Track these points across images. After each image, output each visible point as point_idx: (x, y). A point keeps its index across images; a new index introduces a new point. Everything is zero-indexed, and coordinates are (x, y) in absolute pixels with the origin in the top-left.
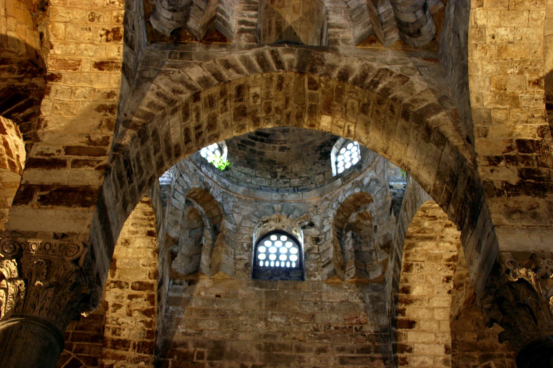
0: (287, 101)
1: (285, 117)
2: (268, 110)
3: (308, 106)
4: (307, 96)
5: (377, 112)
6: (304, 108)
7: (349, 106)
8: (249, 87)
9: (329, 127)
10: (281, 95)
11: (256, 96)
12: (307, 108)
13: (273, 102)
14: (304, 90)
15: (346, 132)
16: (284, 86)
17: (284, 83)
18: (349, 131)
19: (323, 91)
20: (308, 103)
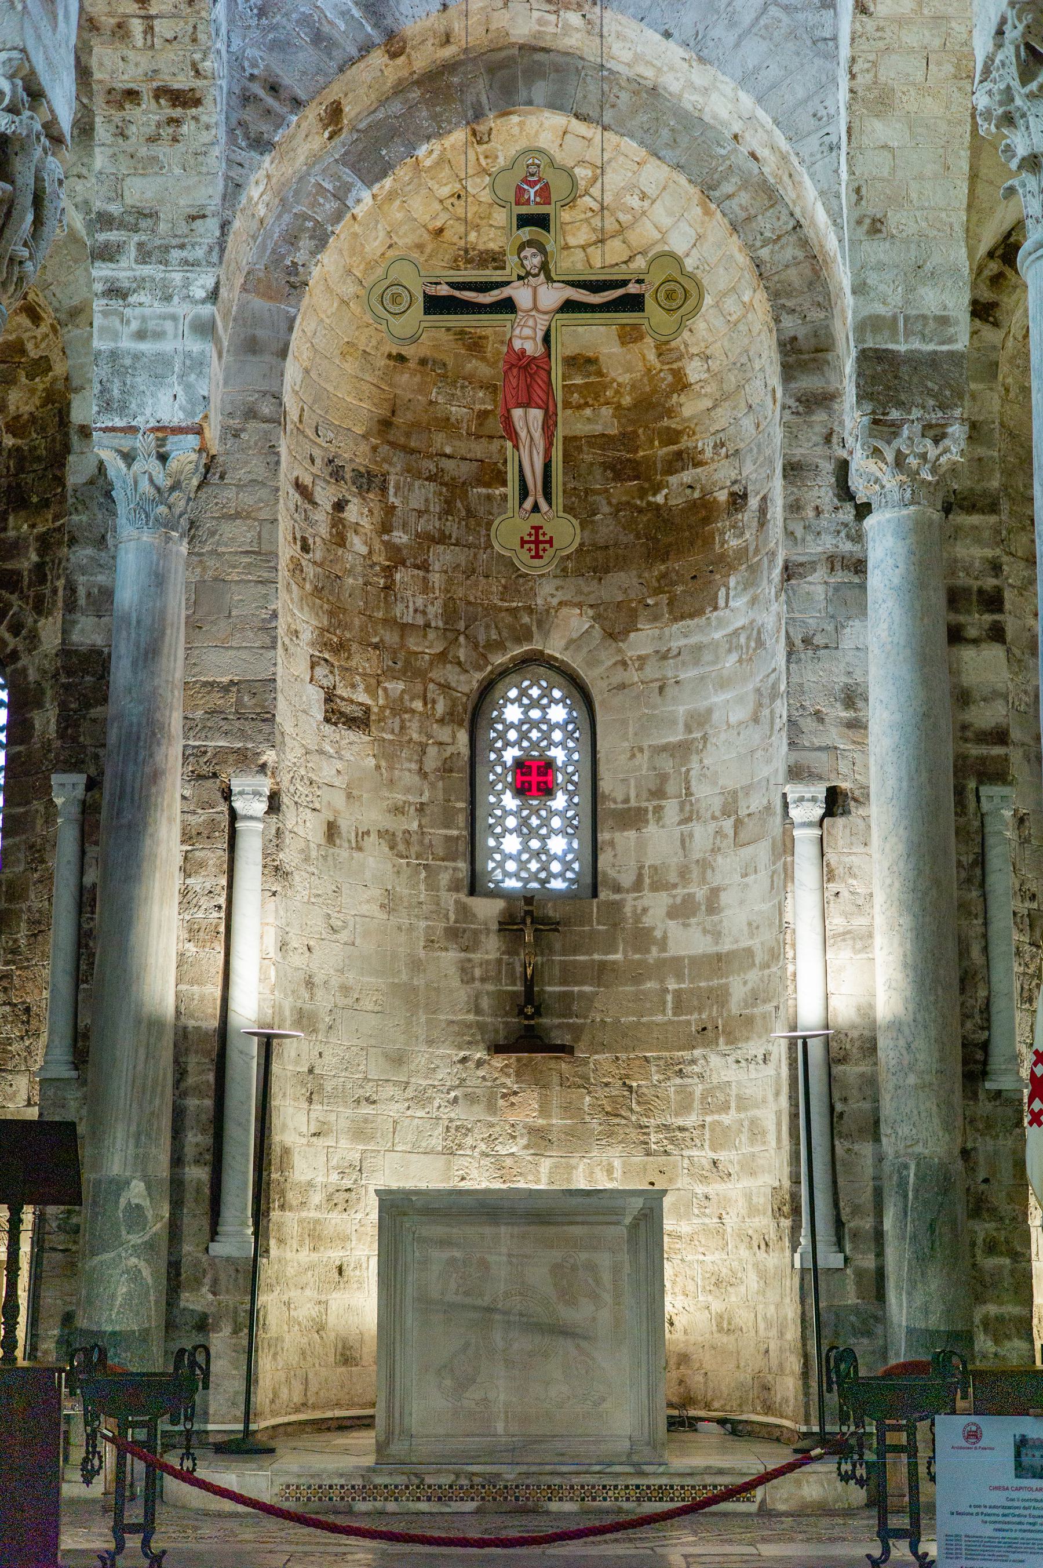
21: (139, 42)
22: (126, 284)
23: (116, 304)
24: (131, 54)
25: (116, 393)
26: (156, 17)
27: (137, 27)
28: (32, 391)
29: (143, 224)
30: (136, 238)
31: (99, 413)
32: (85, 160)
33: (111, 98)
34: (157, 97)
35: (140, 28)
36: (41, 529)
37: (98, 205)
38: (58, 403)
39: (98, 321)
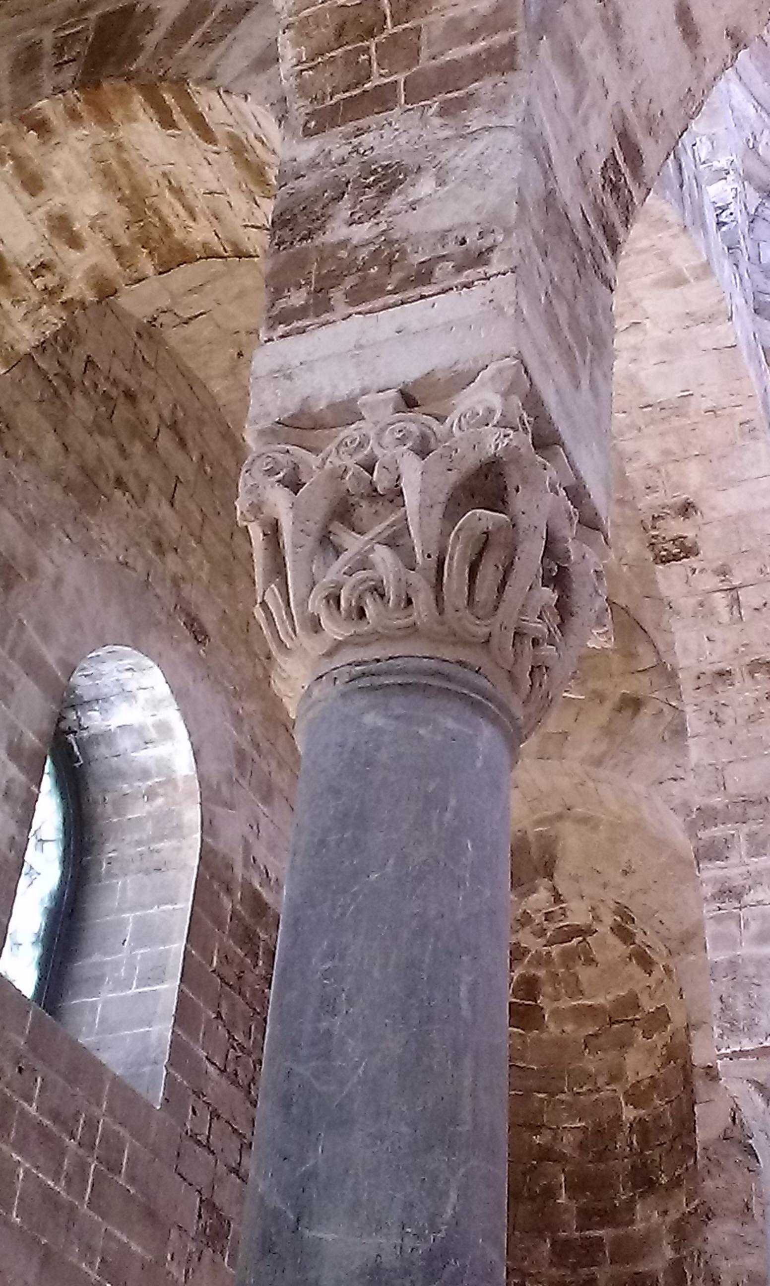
21: (725, 617)
22: (739, 882)
23: (729, 906)
24: (717, 633)
25: (740, 1009)
26: (741, 587)
28: (651, 1051)
29: (752, 811)
30: (745, 828)
31: (721, 1036)
32: (680, 762)
33: (701, 683)
34: (751, 673)
35: (725, 602)
36: (674, 1215)
37: (698, 801)
38: (678, 1055)
39: (710, 929)
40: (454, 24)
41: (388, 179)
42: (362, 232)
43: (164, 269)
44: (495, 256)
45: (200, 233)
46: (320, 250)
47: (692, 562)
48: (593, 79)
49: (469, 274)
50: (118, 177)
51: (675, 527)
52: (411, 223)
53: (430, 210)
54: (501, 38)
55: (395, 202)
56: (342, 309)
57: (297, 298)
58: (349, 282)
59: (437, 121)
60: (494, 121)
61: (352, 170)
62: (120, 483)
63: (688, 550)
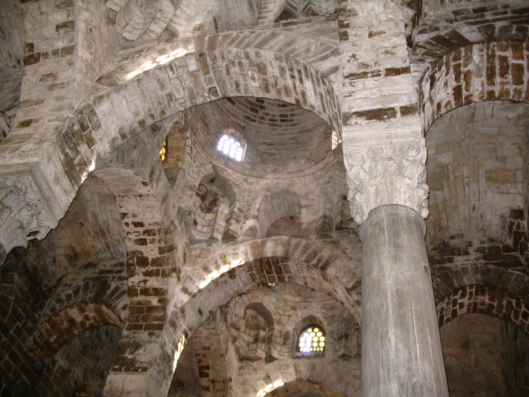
0: (228, 70)
1: (225, 57)
2: (240, 64)
3: (210, 71)
4: (214, 79)
5: (161, 104)
6: (213, 68)
7: (181, 88)
8: (260, 88)
9: (187, 61)
10: (234, 76)
11: (253, 79)
12: (211, 69)
13: (239, 71)
14: (218, 84)
15: (174, 67)
16: (234, 86)
17: (235, 87)
18: (172, 69)
19: (204, 90)
20: (212, 74)
27: (211, 388)
40: (155, 316)
41: (137, 346)
42: (130, 357)
43: (104, 325)
44: (148, 370)
45: (112, 322)
46: (123, 357)
47: (207, 378)
48: (179, 326)
49: (144, 372)
50: (98, 311)
51: (205, 371)
52: (138, 358)
53: (142, 356)
54: (162, 322)
55: (137, 352)
56: (123, 372)
57: (117, 367)
58: (126, 366)
59: (147, 336)
60: (156, 340)
61: (132, 342)
62: (92, 348)
63: (207, 375)
